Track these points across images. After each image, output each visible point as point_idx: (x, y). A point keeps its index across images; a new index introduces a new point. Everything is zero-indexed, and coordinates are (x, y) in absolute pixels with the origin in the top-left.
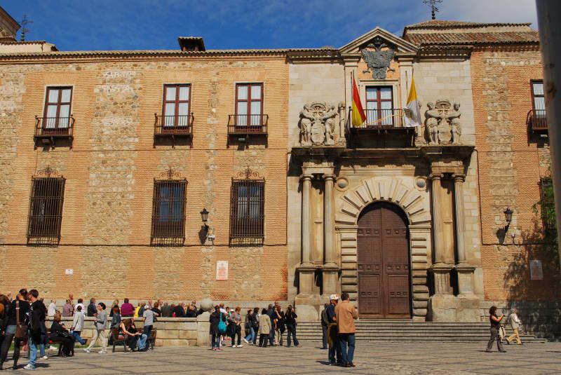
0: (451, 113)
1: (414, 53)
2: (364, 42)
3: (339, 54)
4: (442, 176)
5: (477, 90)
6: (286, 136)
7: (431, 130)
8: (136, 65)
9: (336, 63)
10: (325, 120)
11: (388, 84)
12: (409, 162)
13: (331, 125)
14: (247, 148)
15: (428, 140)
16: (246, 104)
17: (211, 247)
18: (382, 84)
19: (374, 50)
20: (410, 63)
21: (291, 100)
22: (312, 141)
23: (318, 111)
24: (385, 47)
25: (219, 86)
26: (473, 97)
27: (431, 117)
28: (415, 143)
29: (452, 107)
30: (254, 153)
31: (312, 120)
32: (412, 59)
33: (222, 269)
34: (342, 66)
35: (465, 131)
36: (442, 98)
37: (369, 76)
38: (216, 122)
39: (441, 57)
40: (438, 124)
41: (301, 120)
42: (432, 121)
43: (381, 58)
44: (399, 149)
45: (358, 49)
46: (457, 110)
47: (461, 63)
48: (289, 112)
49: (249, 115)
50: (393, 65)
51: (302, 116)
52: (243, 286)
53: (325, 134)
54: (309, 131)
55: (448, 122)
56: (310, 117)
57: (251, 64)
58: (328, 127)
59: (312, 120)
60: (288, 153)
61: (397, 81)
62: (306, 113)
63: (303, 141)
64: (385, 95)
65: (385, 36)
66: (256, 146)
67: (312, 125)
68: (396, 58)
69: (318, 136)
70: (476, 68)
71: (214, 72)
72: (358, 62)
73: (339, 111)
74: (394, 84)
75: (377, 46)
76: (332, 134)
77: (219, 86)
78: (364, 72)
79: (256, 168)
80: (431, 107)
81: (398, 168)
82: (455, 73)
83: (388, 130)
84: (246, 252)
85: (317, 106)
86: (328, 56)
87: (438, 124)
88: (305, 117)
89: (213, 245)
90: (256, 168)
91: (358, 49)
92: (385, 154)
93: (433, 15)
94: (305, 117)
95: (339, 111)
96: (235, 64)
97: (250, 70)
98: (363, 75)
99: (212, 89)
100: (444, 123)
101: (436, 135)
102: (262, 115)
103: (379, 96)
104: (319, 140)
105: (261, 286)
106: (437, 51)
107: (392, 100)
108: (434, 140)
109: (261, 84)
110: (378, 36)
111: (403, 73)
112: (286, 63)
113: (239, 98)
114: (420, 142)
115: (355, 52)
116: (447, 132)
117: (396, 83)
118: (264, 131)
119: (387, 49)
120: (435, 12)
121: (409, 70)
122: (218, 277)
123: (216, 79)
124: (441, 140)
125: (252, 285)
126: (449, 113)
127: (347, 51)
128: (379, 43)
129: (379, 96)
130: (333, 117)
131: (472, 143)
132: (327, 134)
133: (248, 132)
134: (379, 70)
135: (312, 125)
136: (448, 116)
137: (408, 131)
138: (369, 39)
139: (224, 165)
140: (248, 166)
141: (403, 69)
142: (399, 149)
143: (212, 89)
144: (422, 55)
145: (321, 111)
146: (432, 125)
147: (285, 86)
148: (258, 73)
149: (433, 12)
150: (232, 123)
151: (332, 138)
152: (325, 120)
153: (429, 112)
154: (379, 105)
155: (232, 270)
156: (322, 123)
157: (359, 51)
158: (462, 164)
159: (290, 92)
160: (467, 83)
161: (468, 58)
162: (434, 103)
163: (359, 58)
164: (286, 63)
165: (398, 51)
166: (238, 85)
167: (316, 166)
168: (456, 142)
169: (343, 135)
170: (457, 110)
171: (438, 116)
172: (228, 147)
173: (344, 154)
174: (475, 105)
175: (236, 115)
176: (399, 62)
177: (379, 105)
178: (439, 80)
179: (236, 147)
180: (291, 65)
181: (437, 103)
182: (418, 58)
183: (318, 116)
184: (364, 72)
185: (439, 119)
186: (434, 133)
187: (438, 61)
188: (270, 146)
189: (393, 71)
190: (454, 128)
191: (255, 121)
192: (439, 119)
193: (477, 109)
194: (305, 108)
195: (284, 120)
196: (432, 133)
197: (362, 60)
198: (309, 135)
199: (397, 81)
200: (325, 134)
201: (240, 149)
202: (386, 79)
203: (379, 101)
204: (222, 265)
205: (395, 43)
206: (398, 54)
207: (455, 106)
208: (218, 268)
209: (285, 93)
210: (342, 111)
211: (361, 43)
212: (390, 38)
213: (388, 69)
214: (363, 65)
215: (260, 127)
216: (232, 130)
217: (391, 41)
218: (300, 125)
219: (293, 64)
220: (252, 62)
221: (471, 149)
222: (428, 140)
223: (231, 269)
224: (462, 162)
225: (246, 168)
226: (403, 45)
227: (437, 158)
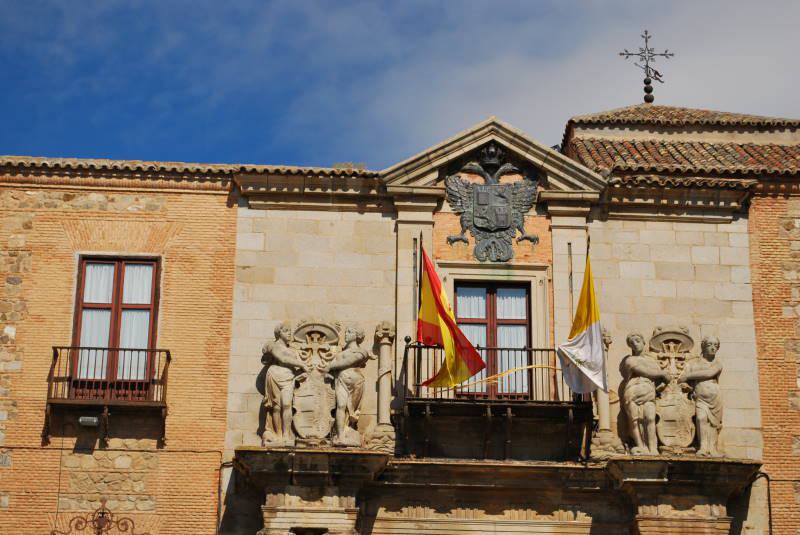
0: (695, 365)
1: (592, 194)
2: (452, 156)
3: (383, 187)
5: (767, 304)
6: (220, 413)
7: (636, 412)
9: (371, 210)
10: (336, 371)
11: (518, 276)
12: (574, 502)
13: (351, 387)
14: (104, 446)
15: (630, 442)
16: (106, 316)
18: (500, 275)
19: (479, 180)
20: (581, 221)
21: (239, 309)
22: (296, 434)
23: (315, 346)
25: (29, 261)
26: (757, 324)
27: (636, 374)
28: (592, 447)
29: (696, 350)
30: (123, 462)
31: (297, 371)
32: (588, 209)
34: (390, 222)
35: (732, 419)
36: (671, 323)
37: (462, 253)
38: (14, 366)
39: (667, 209)
40: (658, 395)
41: (264, 371)
42: (640, 387)
43: (498, 203)
44: (546, 464)
45: (435, 175)
46: (710, 358)
47: (722, 227)
48: (233, 342)
49: (114, 349)
50: (534, 222)
51: (269, 359)
53: (333, 413)
54: (287, 402)
55: (684, 391)
56: (291, 361)
57: (128, 203)
58: (342, 392)
59: (297, 371)
60: (224, 466)
61: (543, 268)
62: (280, 351)
63: (269, 433)
64: (510, 306)
65: (511, 142)
66: (131, 442)
67: (297, 385)
68: (542, 206)
69: (312, 417)
70: (763, 242)
71: (18, 221)
72: (435, 211)
73: (377, 348)
74: (536, 279)
75: (490, 169)
76: (354, 415)
77: (29, 261)
78: (451, 241)
79: (129, 505)
80: (639, 345)
81: (544, 518)
82: (704, 256)
83: (514, 410)
85: (313, 332)
86: (351, 191)
87: (658, 395)
88: (277, 362)
90: (129, 505)
91: (435, 175)
92: (507, 475)
93: (648, 90)
94: (277, 362)
95: (377, 348)
96: (80, 200)
97: (122, 218)
98: (447, 248)
99: (7, 268)
100: (674, 395)
101: (652, 427)
102: (152, 350)
103: (491, 309)
104: (315, 429)
106: (658, 191)
107: (528, 323)
108: (646, 442)
109: (154, 261)
110: (493, 141)
111: (560, 248)
112: (230, 204)
113: (87, 300)
114: (605, 446)
115: (427, 183)
116: (683, 421)
117: (540, 274)
118: (157, 396)
119: (517, 178)
120: (654, 84)
121: (578, 239)
123: (21, 241)
124: (667, 442)
126: (687, 365)
127: (405, 178)
128: (494, 161)
129: (491, 309)
130: (360, 364)
131: (753, 454)
132: (341, 413)
133: (109, 398)
134: (493, 238)
135: (297, 385)
136: (686, 373)
137: (571, 411)
138: (467, 149)
139: (31, 495)
140: (103, 501)
141: (561, 238)
142: (546, 464)
143: (7, 268)
144: (615, 200)
145: (325, 345)
146: (640, 400)
147: (225, 269)
148: (145, 228)
149: (647, 82)
150: (63, 370)
151: (354, 424)
152: (336, 371)
153: (633, 362)
154: (492, 336)
156: (327, 380)
157: (438, 180)
158: (724, 515)
159: (238, 289)
160: (740, 285)
161: (742, 212)
162: (648, 337)
163: (439, 199)
164: (230, 204)
165: (547, 186)
166: (87, 260)
167: (305, 505)
168: (709, 450)
169: (386, 418)
170: (710, 358)
171: (656, 371)
172: (45, 441)
173: (386, 473)
174: (762, 346)
175: (75, 348)
176: (549, 216)
177: (492, 336)
178: (662, 272)
179: (70, 442)
180: (243, 212)
181: (655, 337)
182: (602, 208)
183: (315, 360)
184: (451, 241)
185: (659, 381)
186: (644, 422)
188: (170, 443)
189: (534, 240)
190: (704, 411)
191: (132, 368)
192: (659, 381)
193: (769, 359)
194: (278, 335)
195: (216, 368)
196: (639, 421)
197: (446, 207)
198: (288, 413)
199: (543, 268)
200: (333, 413)
201: (83, 448)
202: (513, 262)
203: (492, 323)
205: (540, 162)
206: (546, 194)
207: (705, 346)
210: (385, 349)
211: (444, 160)
212: (527, 150)
213: (518, 234)
214: (448, 221)
215: (144, 386)
216: (62, 391)
217: (529, 156)
218: (261, 383)
219: (250, 207)
220: (131, 198)
221: (748, 472)
222: (630, 442)
224: (724, 509)
225: (98, 505)
226: (561, 169)
227: (655, 496)
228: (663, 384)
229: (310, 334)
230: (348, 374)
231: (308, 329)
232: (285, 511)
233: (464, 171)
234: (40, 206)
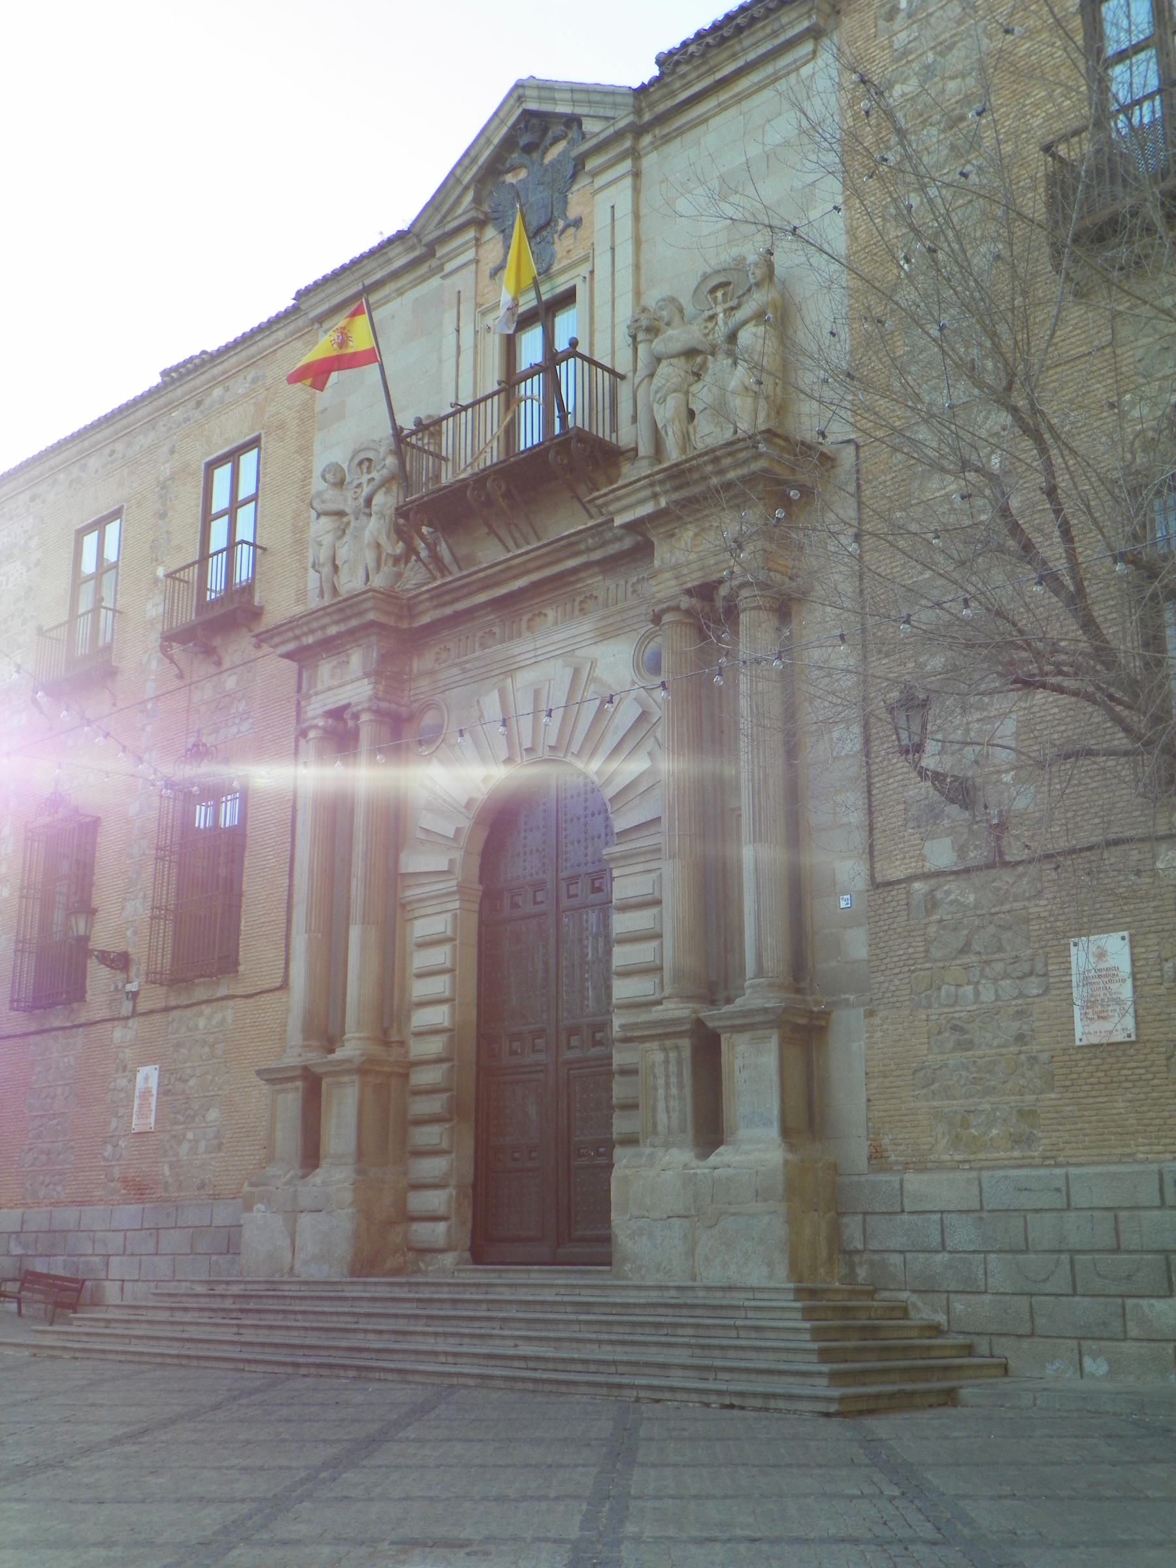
4: (685, 602)
8: (33, 499)
10: (369, 502)
17: (131, 1022)
24: (556, 140)
33: (146, 1093)
52: (185, 1147)
61: (585, 259)
71: (165, 449)
84: (196, 1028)
89: (134, 1014)
91: (469, 196)
96: (207, 402)
100: (718, 365)
105: (219, 1147)
109: (255, 443)
122: (136, 1125)
125: (202, 1145)
127: (438, 218)
155: (167, 1093)
157: (477, 200)
187: (723, 108)
199: (585, 259)
204: (146, 1079)
208: (137, 1094)
209: (305, 450)
211: (475, 169)
223: (165, 1091)
228: (699, 359)
229: (360, 463)
230: (378, 499)
231: (356, 461)
232: (317, 694)
233: (508, 172)
234: (179, 425)
